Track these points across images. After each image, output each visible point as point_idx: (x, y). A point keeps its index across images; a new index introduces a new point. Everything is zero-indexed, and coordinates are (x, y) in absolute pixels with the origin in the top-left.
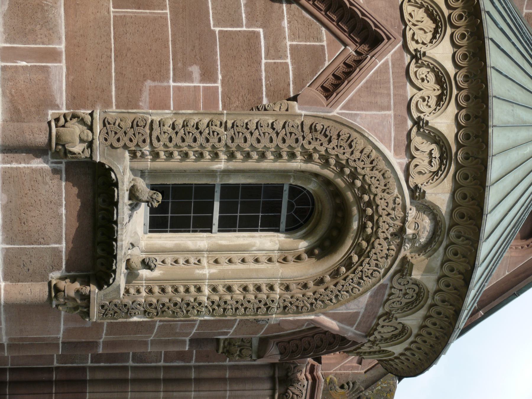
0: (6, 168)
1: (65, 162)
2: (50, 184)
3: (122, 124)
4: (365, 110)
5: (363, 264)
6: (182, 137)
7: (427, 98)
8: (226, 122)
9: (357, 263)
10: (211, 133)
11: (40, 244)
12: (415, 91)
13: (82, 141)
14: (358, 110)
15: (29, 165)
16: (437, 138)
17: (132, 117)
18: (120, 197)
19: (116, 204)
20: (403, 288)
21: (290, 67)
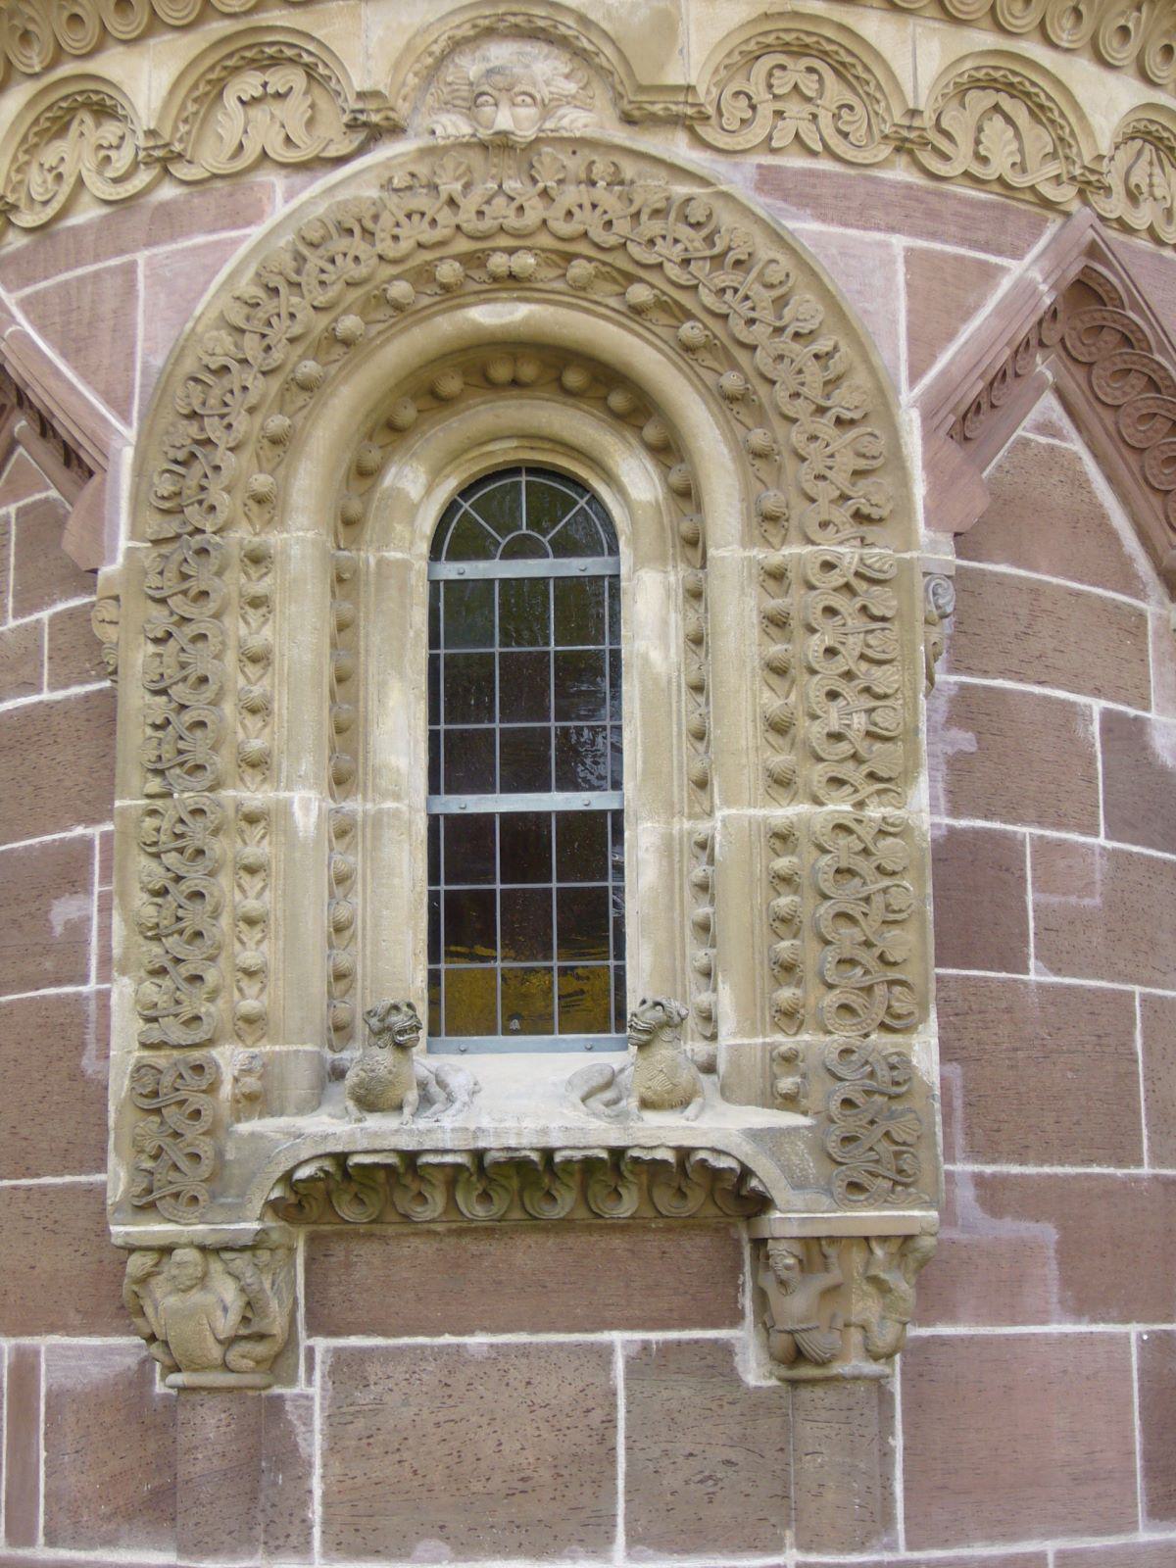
0: (324, 1542)
1: (309, 1336)
2: (379, 1389)
3: (150, 1147)
4: (133, 346)
5: (652, 259)
6: (189, 942)
7: (102, 153)
8: (149, 796)
9: (653, 286)
10: (180, 843)
11: (610, 1421)
12: (85, 198)
13: (202, 1281)
14: (133, 369)
15: (318, 1461)
16: (205, 89)
17: (132, 1115)
18: (377, 1145)
19: (410, 1157)
20: (766, 110)
21: (60, 607)
